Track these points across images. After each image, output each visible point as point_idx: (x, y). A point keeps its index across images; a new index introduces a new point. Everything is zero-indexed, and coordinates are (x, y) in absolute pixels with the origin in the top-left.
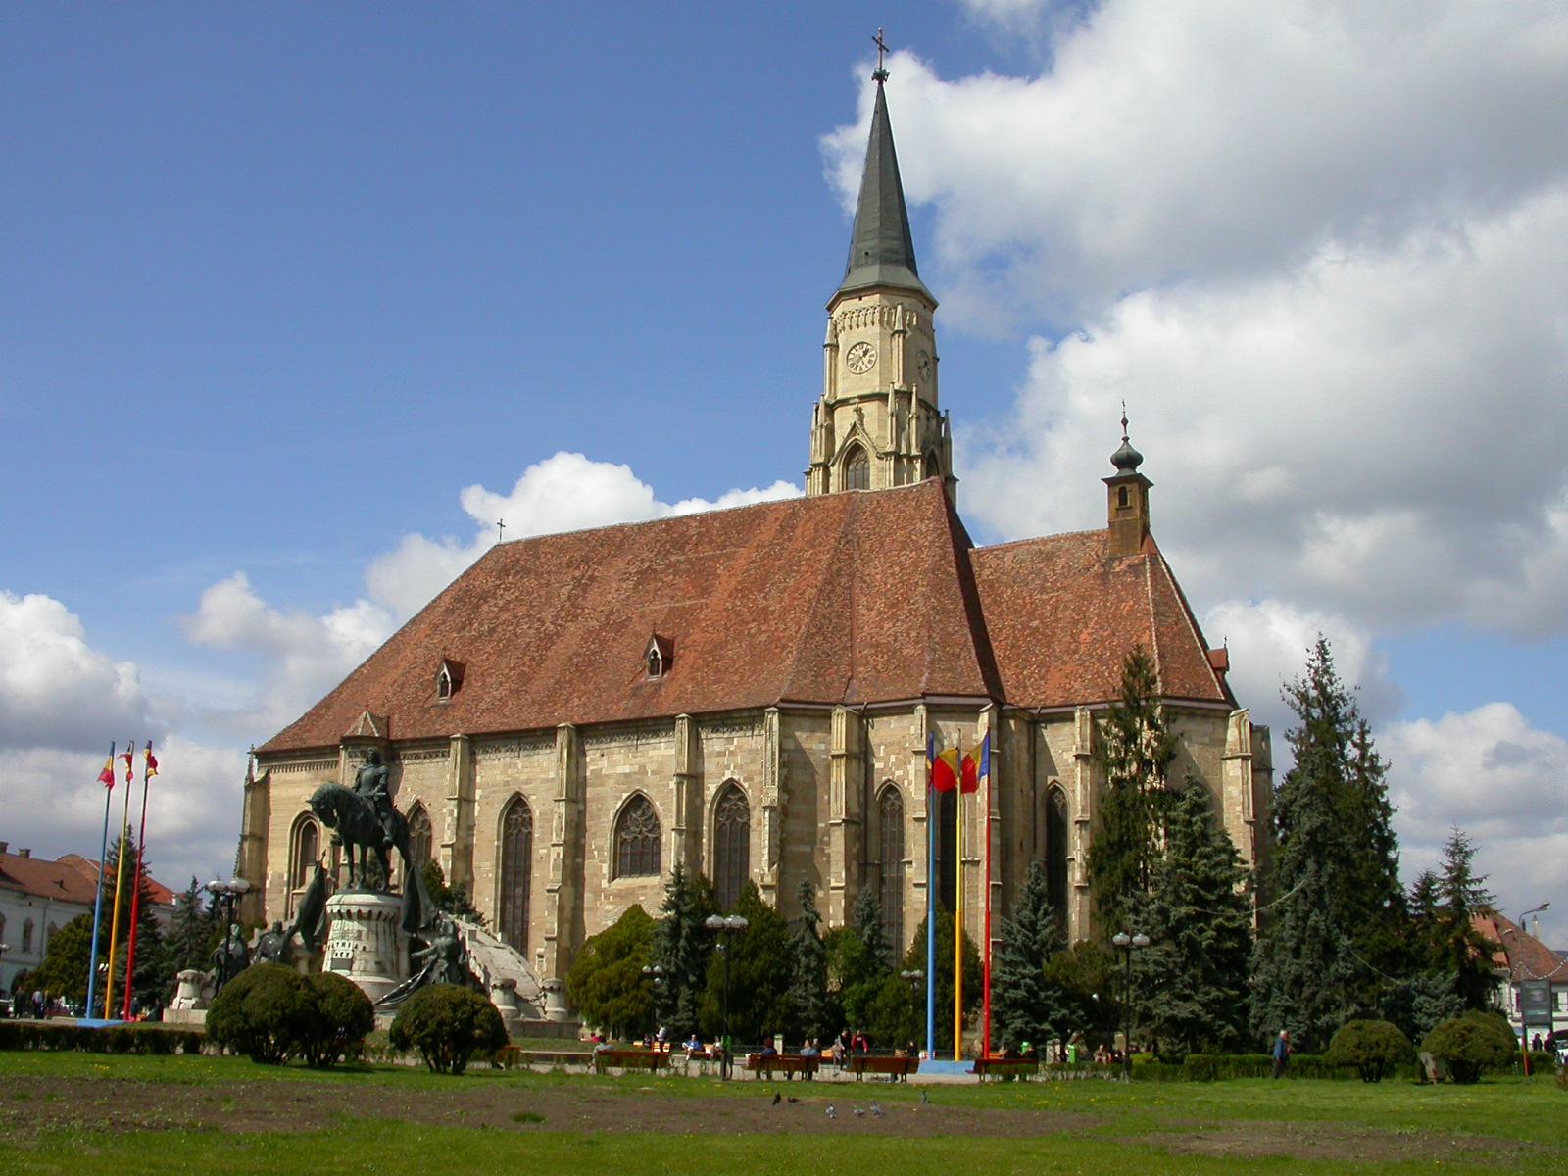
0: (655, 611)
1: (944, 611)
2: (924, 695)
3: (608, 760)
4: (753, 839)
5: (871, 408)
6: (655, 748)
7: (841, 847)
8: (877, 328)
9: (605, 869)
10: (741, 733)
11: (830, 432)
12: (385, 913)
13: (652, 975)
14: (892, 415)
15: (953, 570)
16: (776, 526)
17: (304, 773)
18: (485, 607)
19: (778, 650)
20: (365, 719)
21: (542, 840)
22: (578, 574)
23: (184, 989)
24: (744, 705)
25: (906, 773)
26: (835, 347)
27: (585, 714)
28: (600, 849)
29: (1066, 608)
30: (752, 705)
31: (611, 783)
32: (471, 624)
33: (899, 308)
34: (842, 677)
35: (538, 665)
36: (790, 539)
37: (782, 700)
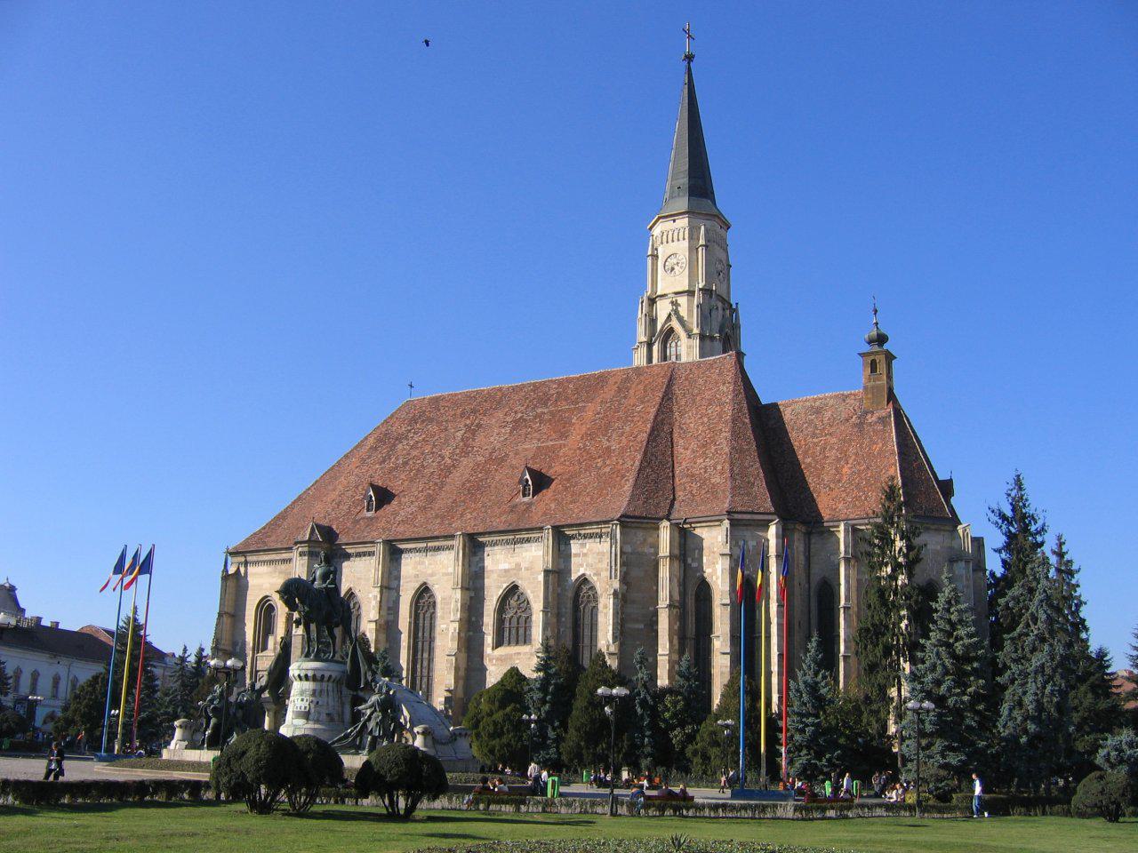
0: (526, 450)
1: (741, 451)
2: (729, 513)
4: (601, 619)
5: (683, 300)
6: (527, 551)
7: (667, 626)
8: (686, 244)
11: (653, 321)
12: (334, 676)
13: (530, 721)
14: (698, 306)
15: (747, 421)
16: (615, 388)
17: (265, 567)
18: (400, 446)
19: (618, 479)
20: (313, 529)
21: (443, 618)
22: (468, 422)
23: (178, 733)
24: (594, 520)
26: (655, 257)
27: (475, 525)
29: (832, 448)
30: (598, 520)
31: (494, 576)
32: (390, 459)
33: (703, 228)
34: (667, 499)
35: (440, 489)
36: (625, 397)
37: (622, 516)
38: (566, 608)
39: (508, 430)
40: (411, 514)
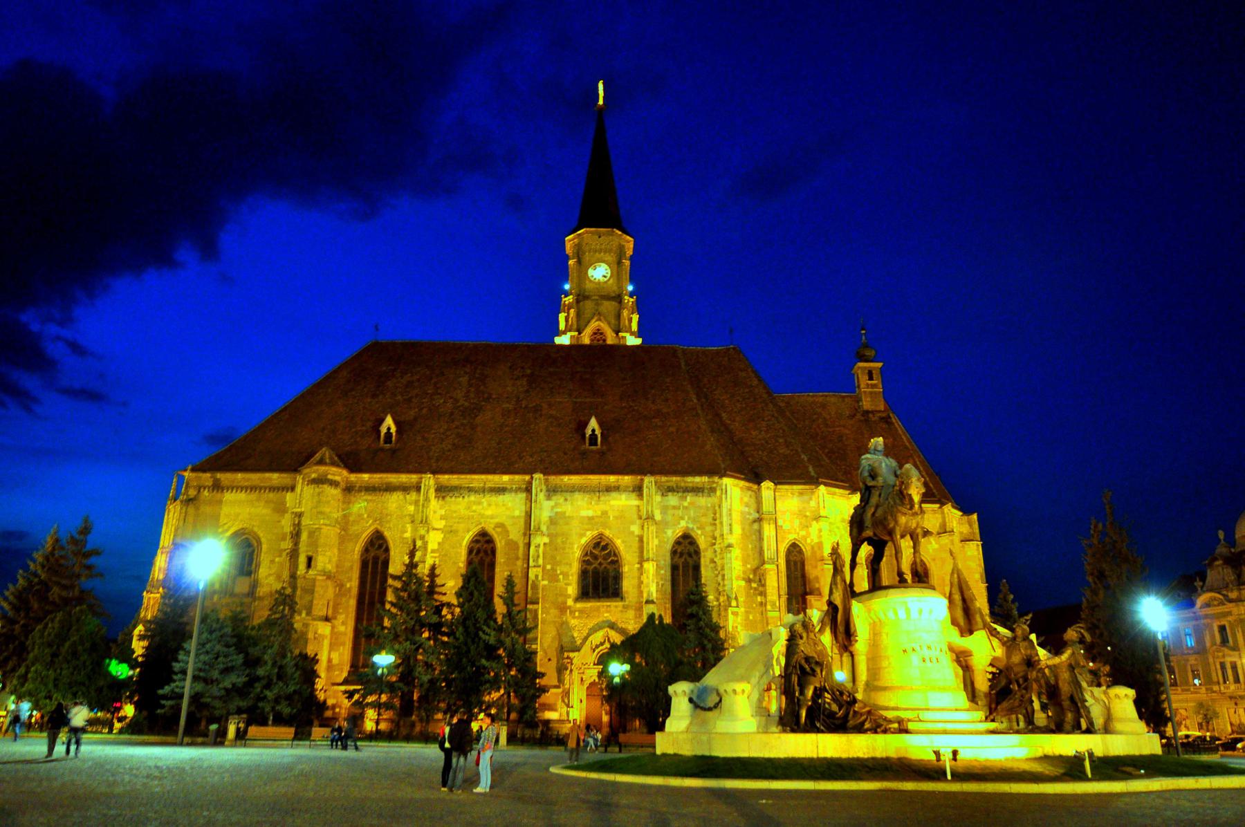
0: (560, 402)
3: (572, 504)
9: (572, 590)
25: (809, 534)
28: (566, 575)
38: (665, 560)
40: (449, 451)
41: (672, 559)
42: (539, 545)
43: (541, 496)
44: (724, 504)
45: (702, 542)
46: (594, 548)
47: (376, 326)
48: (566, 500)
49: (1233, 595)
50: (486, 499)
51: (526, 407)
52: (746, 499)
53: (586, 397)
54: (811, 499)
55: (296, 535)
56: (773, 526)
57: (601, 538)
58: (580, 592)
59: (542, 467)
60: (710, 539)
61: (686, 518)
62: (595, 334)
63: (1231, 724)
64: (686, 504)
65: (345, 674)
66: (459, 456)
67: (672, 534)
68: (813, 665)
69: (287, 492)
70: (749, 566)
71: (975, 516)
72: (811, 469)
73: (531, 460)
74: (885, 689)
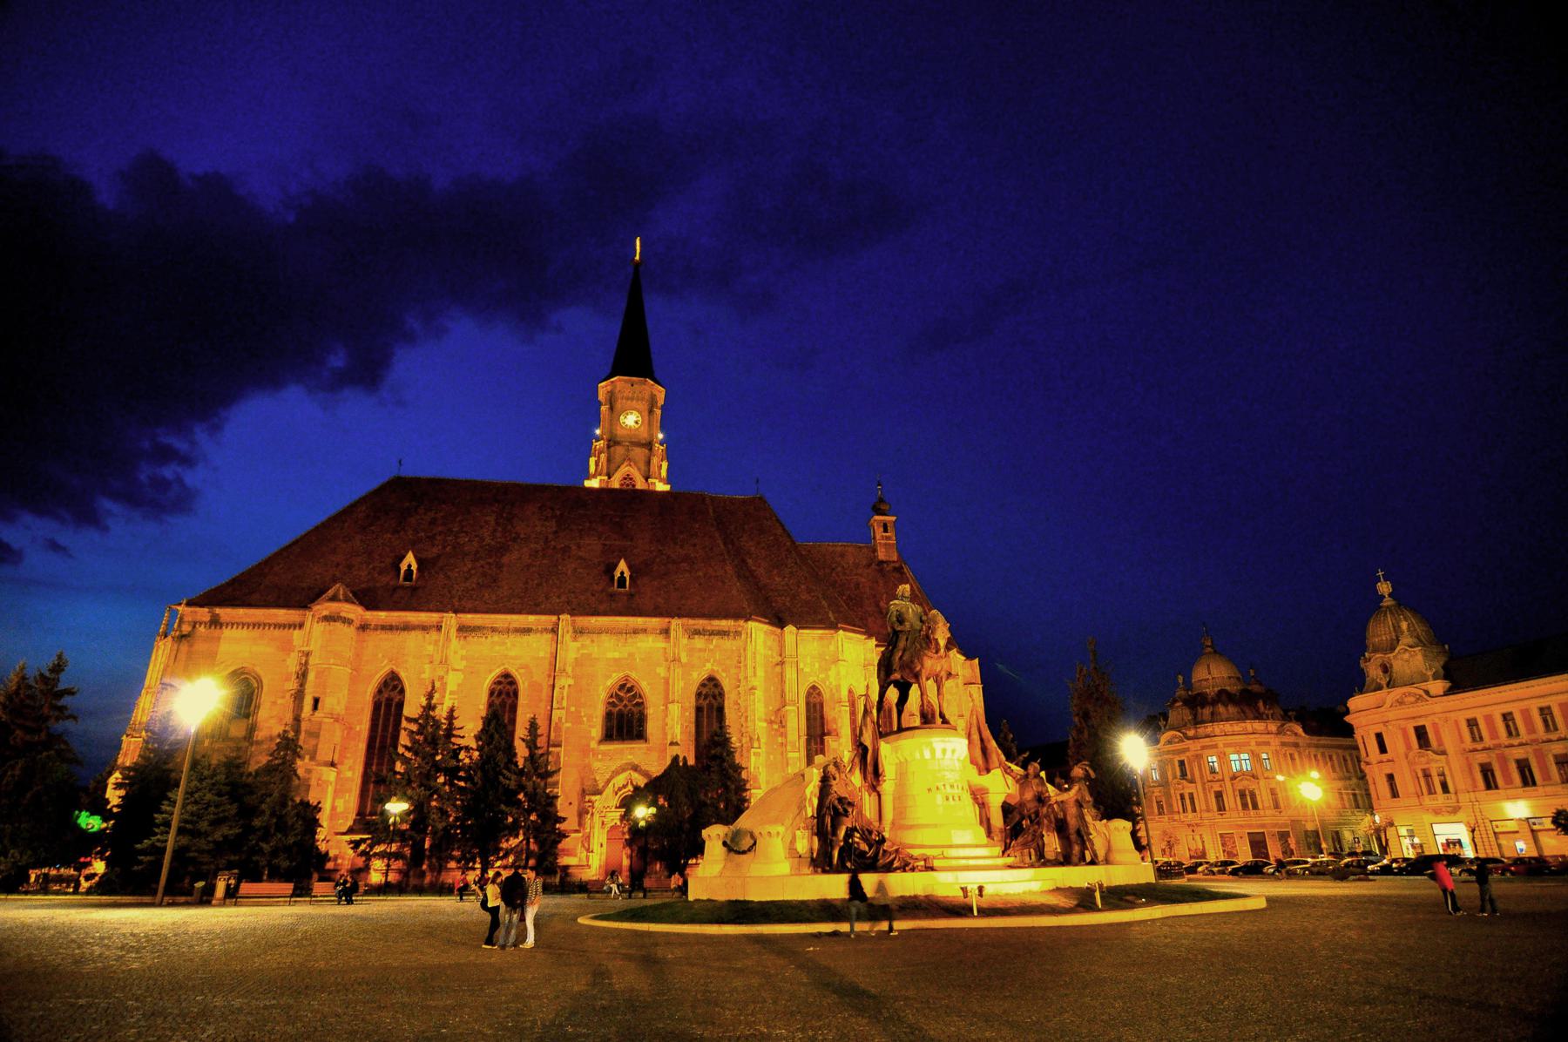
0: (589, 545)
9: (597, 731)
10: (717, 637)
25: (827, 677)
28: (590, 717)
39: (553, 523)
41: (697, 700)
42: (564, 686)
43: (568, 637)
44: (749, 648)
45: (726, 684)
46: (619, 690)
47: (400, 462)
48: (593, 641)
49: (1191, 733)
50: (512, 639)
51: (555, 547)
52: (769, 643)
53: (615, 540)
54: (830, 643)
55: (302, 676)
56: (794, 670)
57: (627, 680)
58: (604, 732)
59: (569, 608)
60: (734, 682)
61: (712, 661)
62: (625, 479)
63: (1189, 849)
64: (712, 647)
65: (350, 823)
66: (484, 596)
67: (698, 676)
68: (846, 806)
69: (295, 628)
70: (771, 708)
71: (977, 661)
72: (831, 615)
73: (557, 601)
74: (911, 827)
